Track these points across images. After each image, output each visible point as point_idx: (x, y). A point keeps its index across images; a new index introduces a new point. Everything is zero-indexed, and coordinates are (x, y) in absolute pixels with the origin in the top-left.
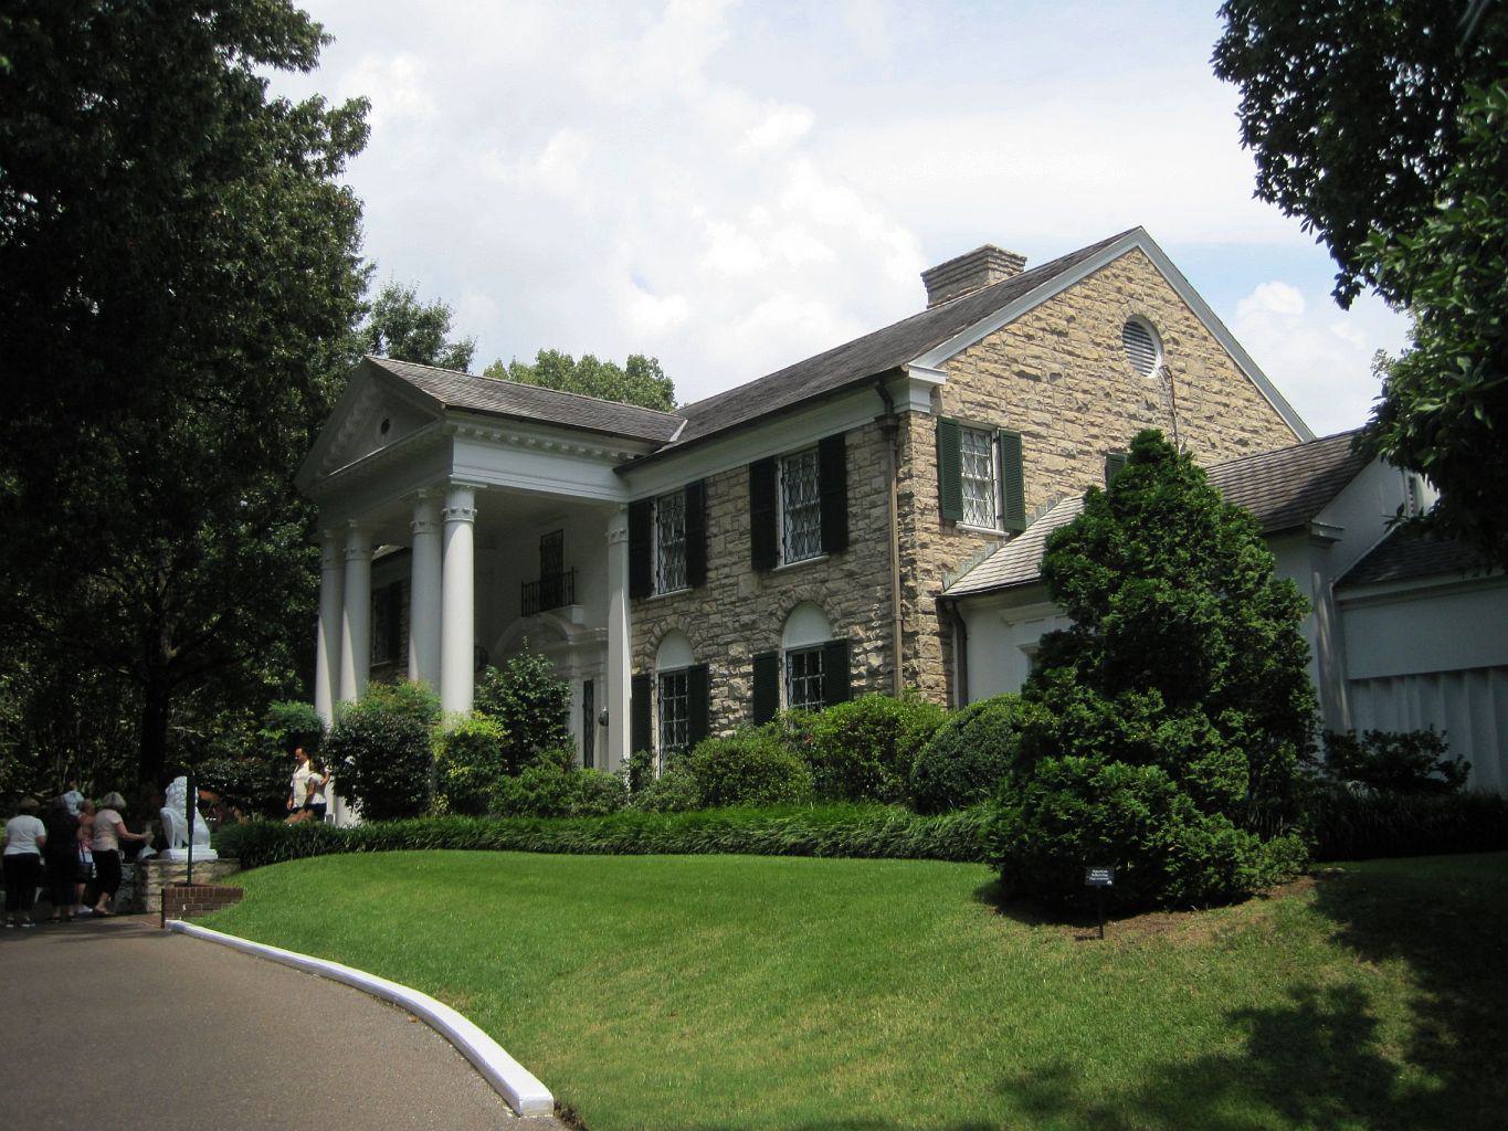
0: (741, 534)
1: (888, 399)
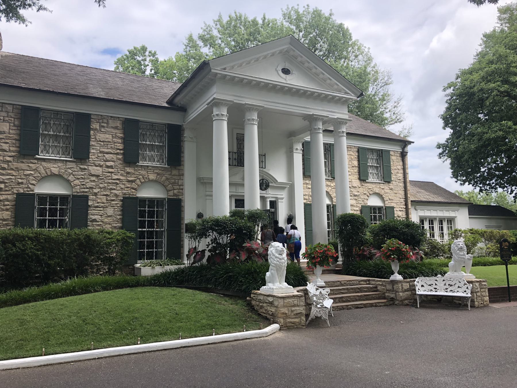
0: (353, 167)
1: (403, 149)
